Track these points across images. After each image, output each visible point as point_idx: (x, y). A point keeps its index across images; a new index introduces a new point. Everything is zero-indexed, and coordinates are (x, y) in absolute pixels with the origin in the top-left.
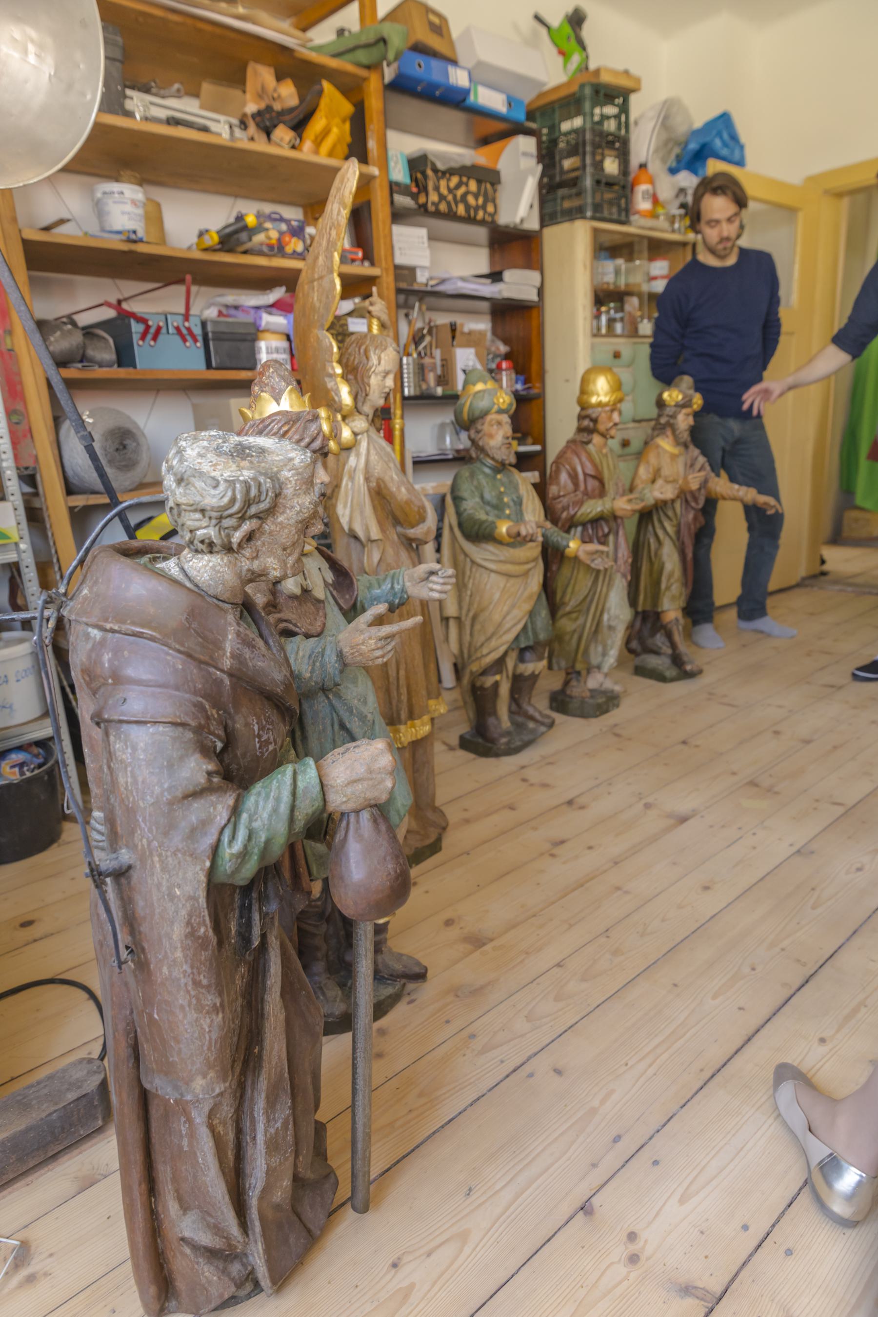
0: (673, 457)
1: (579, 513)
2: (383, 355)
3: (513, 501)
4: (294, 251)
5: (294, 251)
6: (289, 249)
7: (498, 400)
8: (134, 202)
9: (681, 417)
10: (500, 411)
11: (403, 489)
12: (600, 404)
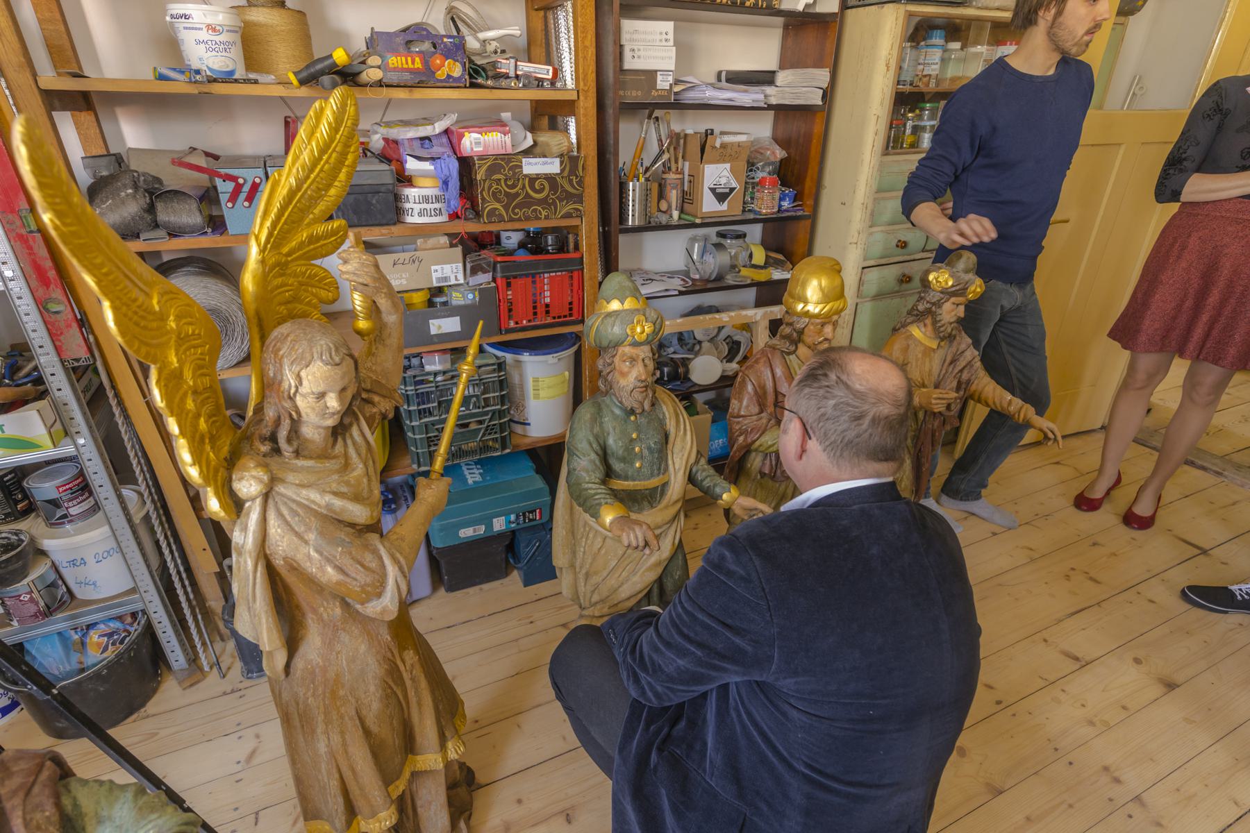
0: (928, 351)
1: (757, 443)
3: (649, 448)
4: (449, 76)
5: (449, 76)
6: (441, 74)
7: (633, 330)
8: (211, 28)
9: (947, 306)
10: (635, 344)
11: (329, 569)
12: (807, 314)
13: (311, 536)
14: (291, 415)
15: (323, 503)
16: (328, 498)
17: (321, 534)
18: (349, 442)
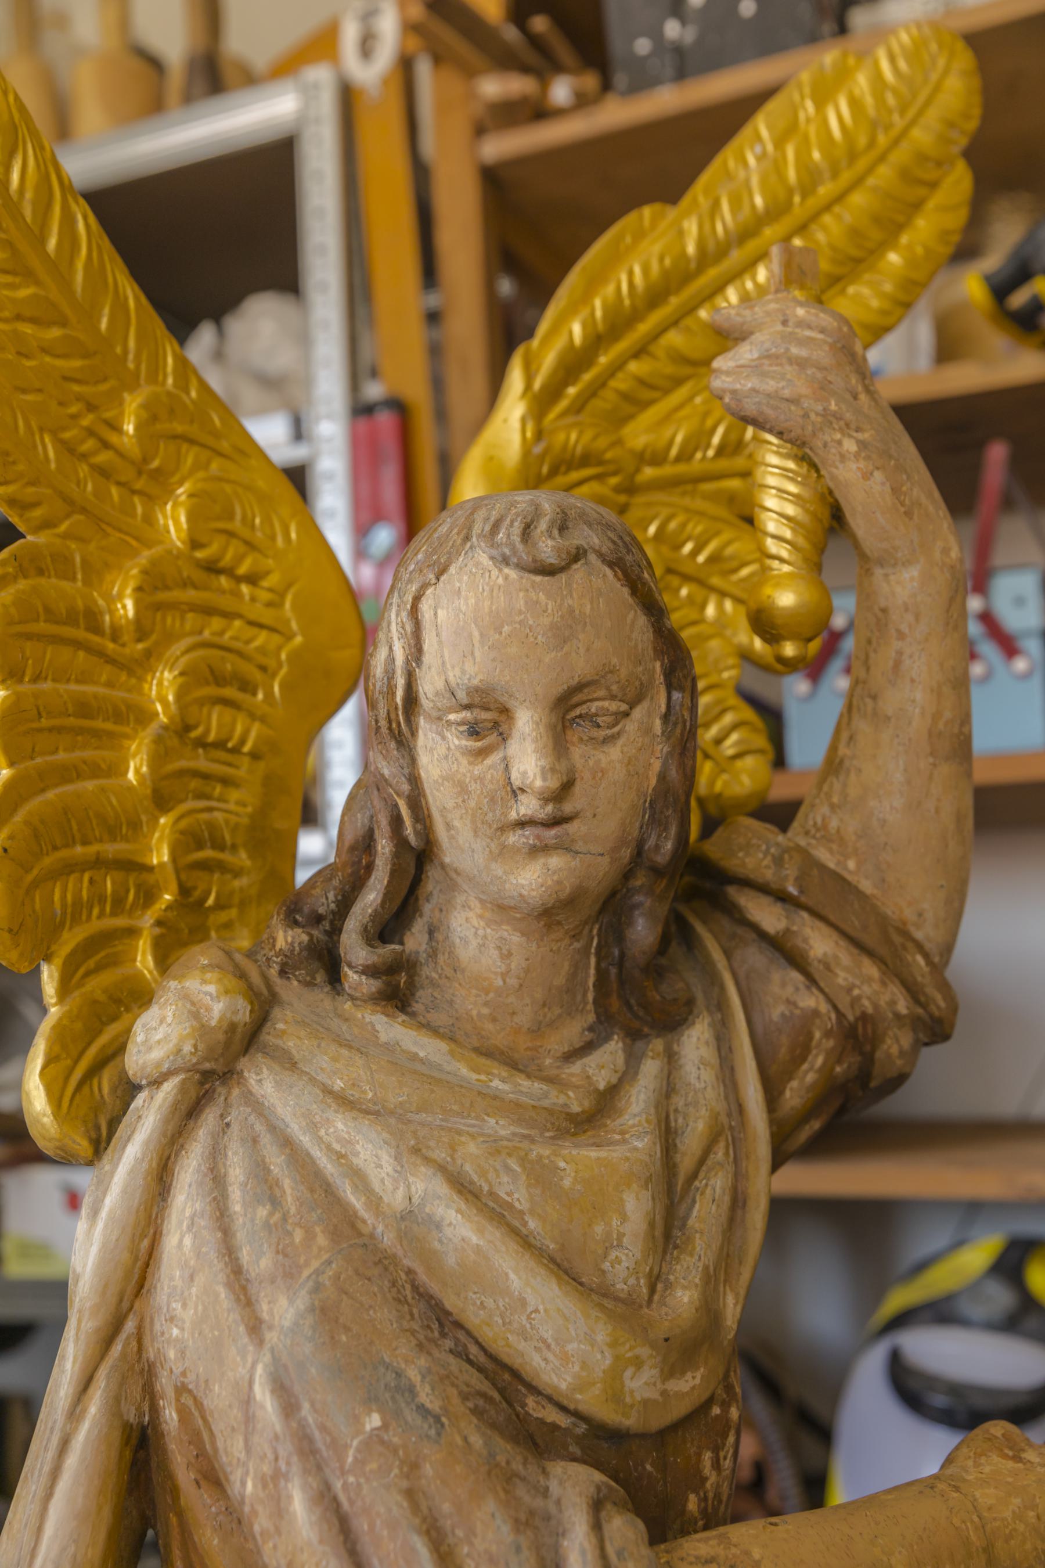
2: (426, 607)
11: (299, 1504)
13: (284, 1310)
14: (396, 821)
16: (424, 1186)
17: (325, 1314)
18: (650, 1068)
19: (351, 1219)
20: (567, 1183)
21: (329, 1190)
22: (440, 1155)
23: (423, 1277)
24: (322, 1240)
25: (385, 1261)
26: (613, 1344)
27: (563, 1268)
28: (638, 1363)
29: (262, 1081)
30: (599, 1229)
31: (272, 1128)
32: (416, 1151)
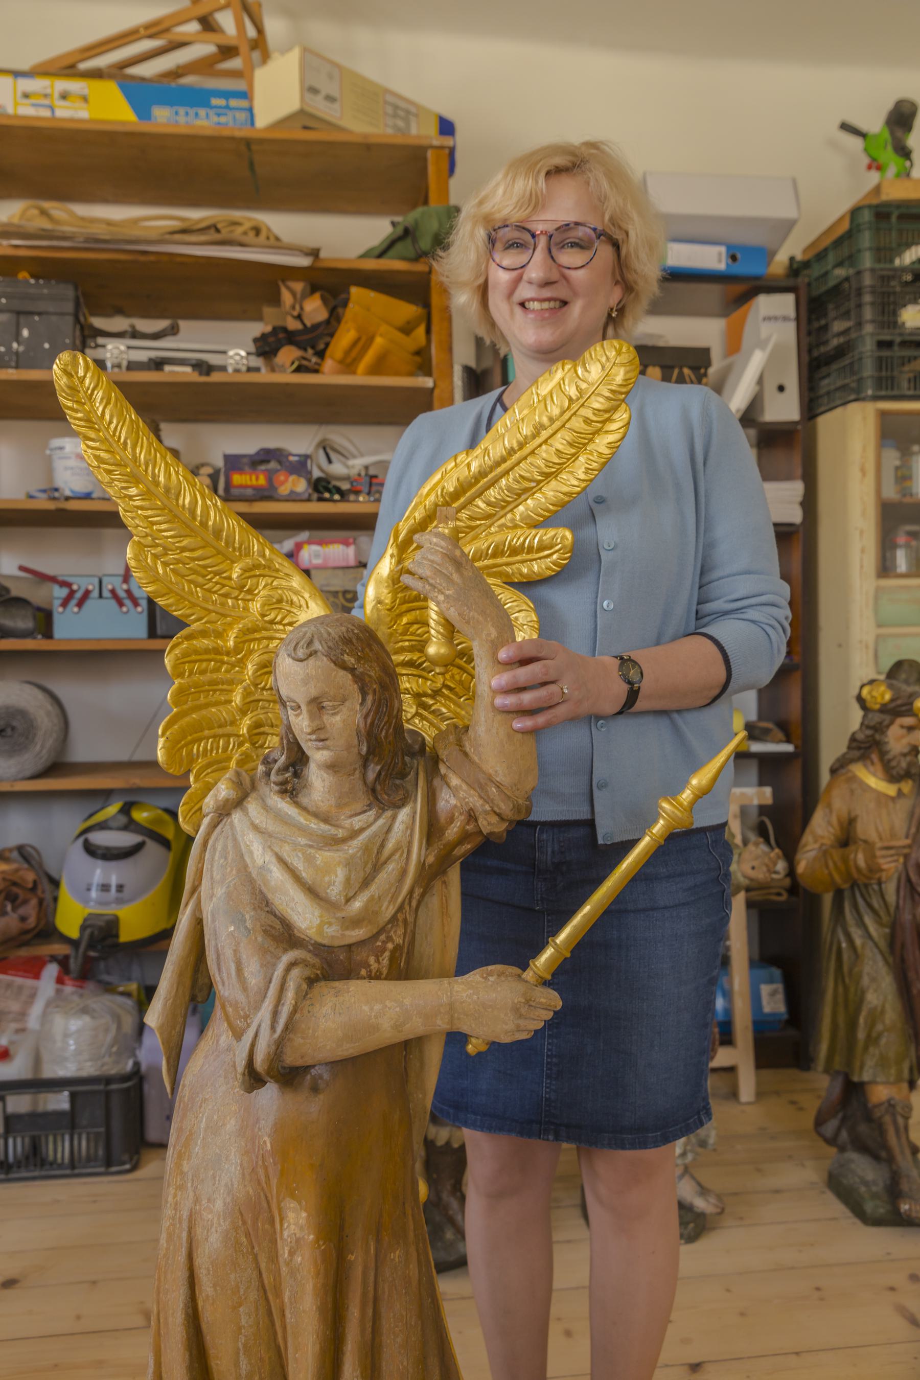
15: (259, 862)
16: (269, 858)
17: (229, 895)
19: (246, 866)
20: (318, 862)
21: (242, 856)
22: (277, 849)
23: (263, 888)
24: (234, 872)
25: (251, 881)
26: (321, 917)
27: (312, 892)
28: (330, 924)
29: (236, 816)
30: (327, 879)
31: (233, 834)
32: (270, 847)
